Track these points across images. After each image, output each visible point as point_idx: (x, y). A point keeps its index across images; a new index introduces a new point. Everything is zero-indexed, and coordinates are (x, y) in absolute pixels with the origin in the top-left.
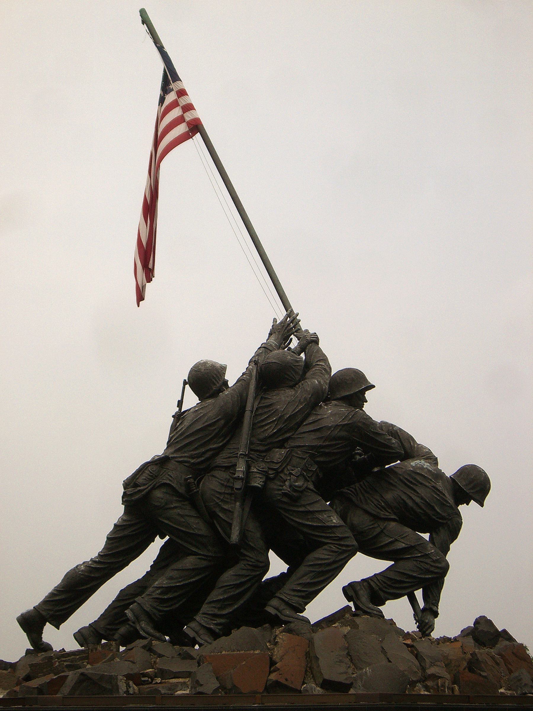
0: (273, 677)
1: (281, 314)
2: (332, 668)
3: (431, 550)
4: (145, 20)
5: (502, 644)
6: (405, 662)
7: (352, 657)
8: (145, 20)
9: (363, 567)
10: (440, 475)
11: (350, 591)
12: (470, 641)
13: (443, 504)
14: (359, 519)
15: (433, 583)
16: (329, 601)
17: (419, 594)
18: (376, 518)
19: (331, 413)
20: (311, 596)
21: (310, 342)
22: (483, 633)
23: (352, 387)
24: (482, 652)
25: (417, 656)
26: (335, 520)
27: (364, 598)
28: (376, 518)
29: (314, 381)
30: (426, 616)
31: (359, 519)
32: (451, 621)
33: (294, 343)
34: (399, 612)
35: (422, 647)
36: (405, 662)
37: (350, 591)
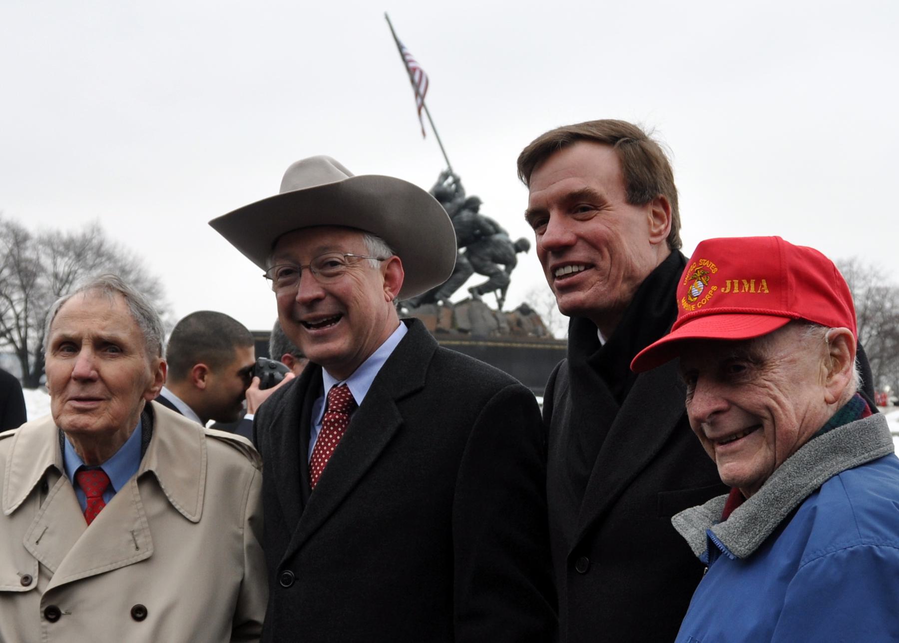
0: (439, 326)
1: (445, 168)
2: (463, 323)
3: (505, 274)
4: (387, 18)
5: (532, 315)
6: (492, 322)
7: (471, 318)
8: (387, 18)
9: (477, 279)
10: (509, 242)
11: (471, 290)
12: (519, 315)
13: (510, 254)
14: (476, 260)
15: (504, 288)
16: (461, 294)
17: (499, 292)
18: (482, 260)
19: (466, 215)
20: (453, 291)
21: (457, 181)
22: (525, 310)
23: (473, 204)
24: (524, 319)
25: (497, 319)
26: (465, 261)
27: (476, 292)
28: (482, 260)
29: (459, 200)
30: (501, 301)
31: (476, 260)
32: (511, 304)
33: (450, 180)
34: (490, 299)
35: (499, 316)
36: (492, 322)
37: (471, 290)
